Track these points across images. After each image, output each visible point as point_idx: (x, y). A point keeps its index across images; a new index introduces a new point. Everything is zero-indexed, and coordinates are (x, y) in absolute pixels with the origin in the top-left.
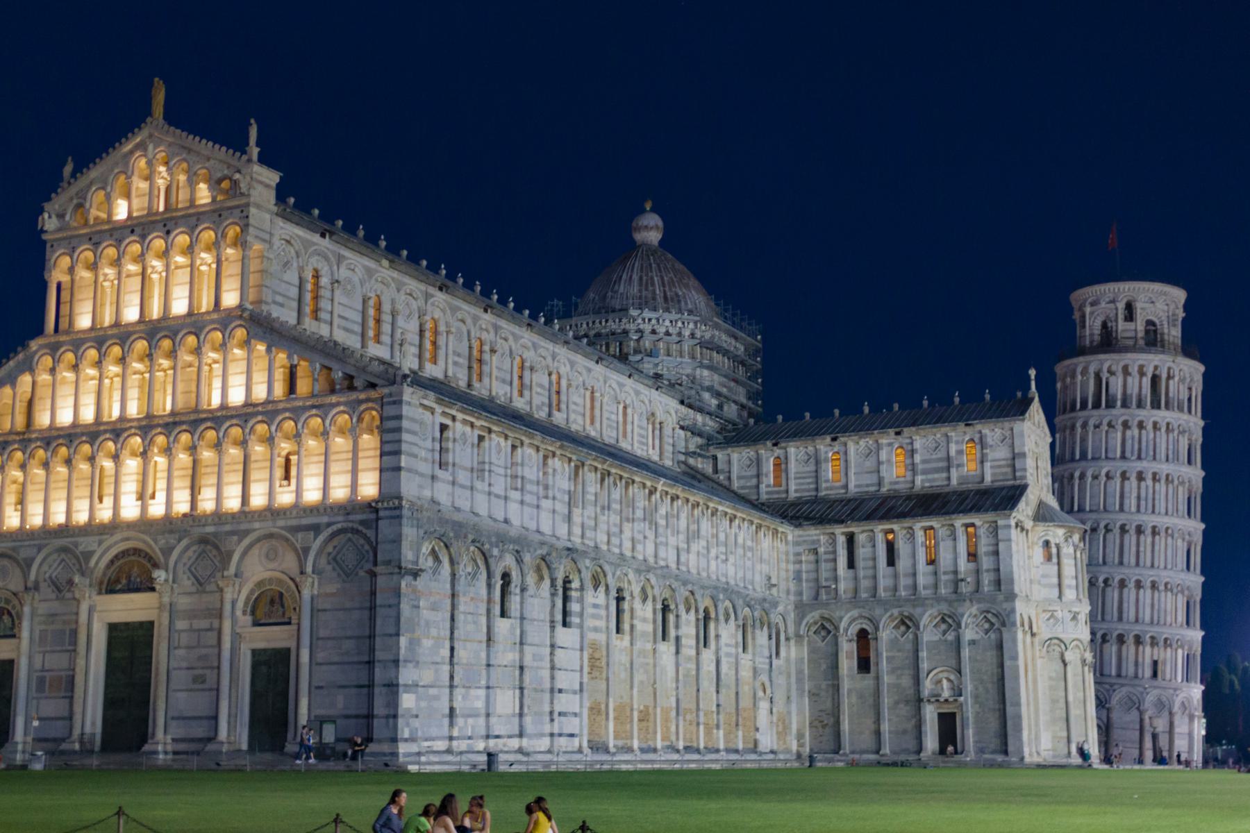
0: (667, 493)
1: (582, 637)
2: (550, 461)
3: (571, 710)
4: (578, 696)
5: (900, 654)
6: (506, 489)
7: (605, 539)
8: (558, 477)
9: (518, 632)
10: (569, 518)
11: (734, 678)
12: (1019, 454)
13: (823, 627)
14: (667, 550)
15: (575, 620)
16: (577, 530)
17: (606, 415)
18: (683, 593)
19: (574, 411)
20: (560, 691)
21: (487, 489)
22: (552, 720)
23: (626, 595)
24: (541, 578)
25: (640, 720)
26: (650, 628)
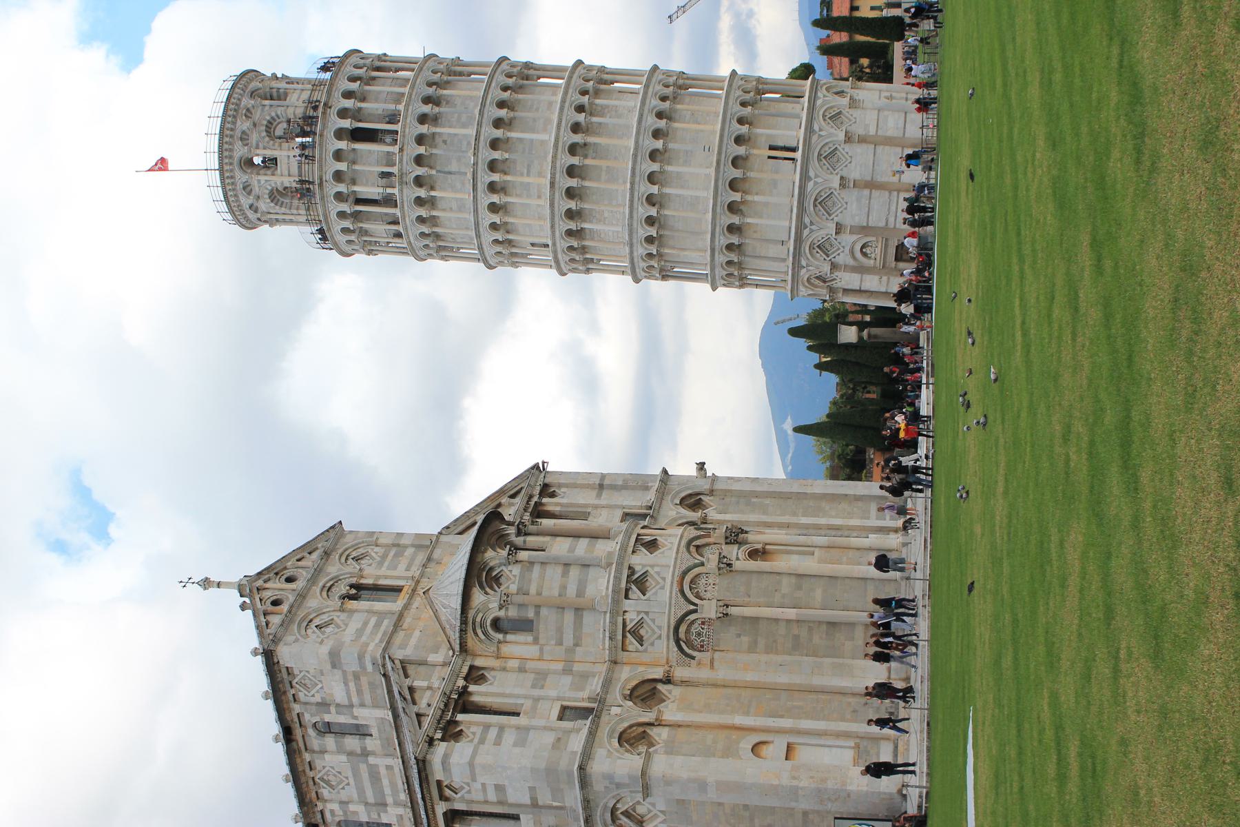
12: (334, 666)
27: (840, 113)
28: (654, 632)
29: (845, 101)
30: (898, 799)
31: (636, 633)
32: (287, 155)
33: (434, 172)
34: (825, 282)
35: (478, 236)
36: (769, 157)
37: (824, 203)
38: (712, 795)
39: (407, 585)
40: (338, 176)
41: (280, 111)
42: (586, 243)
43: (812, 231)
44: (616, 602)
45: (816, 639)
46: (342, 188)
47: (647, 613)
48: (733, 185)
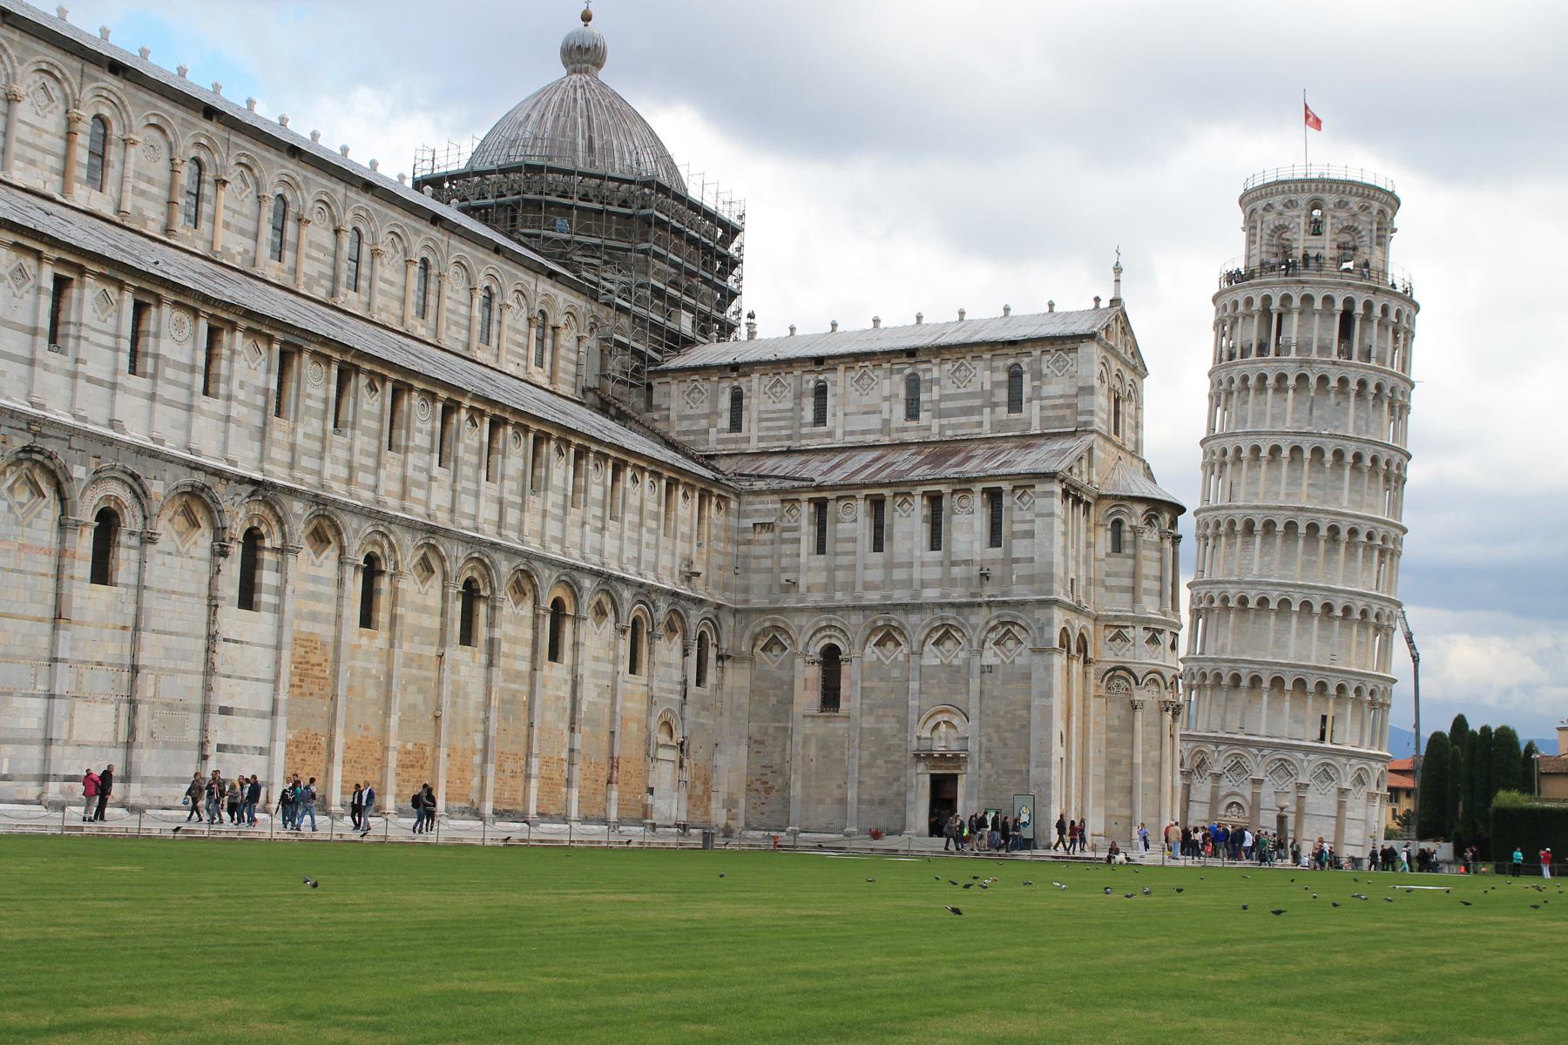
0: (482, 413)
1: (280, 627)
2: (225, 337)
3: (251, 743)
4: (267, 722)
5: (883, 684)
6: (116, 372)
7: (343, 472)
8: (240, 365)
9: (132, 609)
10: (263, 433)
11: (607, 711)
12: (1081, 389)
13: (775, 639)
14: (477, 504)
15: (265, 598)
16: (280, 454)
17: (447, 303)
18: (505, 568)
19: (384, 293)
20: (225, 711)
21: (70, 367)
22: (205, 757)
23: (387, 567)
24: (195, 524)
25: (402, 766)
26: (434, 622)
27: (1363, 784)
28: (1121, 649)
29: (1373, 789)
30: (1044, 843)
31: (1119, 636)
32: (1326, 246)
33: (1312, 394)
34: (1198, 767)
35: (1246, 434)
36: (1324, 718)
37: (1283, 768)
38: (1037, 702)
39: (1118, 440)
40: (1308, 299)
41: (1366, 239)
42: (1239, 540)
43: (1256, 756)
44: (1142, 620)
45: (1118, 778)
46: (1296, 302)
47: (1134, 645)
48: (1300, 683)
